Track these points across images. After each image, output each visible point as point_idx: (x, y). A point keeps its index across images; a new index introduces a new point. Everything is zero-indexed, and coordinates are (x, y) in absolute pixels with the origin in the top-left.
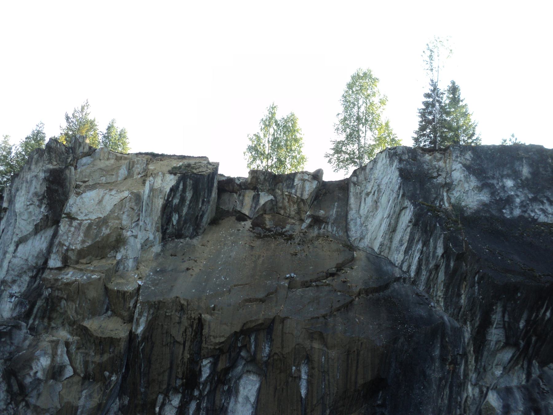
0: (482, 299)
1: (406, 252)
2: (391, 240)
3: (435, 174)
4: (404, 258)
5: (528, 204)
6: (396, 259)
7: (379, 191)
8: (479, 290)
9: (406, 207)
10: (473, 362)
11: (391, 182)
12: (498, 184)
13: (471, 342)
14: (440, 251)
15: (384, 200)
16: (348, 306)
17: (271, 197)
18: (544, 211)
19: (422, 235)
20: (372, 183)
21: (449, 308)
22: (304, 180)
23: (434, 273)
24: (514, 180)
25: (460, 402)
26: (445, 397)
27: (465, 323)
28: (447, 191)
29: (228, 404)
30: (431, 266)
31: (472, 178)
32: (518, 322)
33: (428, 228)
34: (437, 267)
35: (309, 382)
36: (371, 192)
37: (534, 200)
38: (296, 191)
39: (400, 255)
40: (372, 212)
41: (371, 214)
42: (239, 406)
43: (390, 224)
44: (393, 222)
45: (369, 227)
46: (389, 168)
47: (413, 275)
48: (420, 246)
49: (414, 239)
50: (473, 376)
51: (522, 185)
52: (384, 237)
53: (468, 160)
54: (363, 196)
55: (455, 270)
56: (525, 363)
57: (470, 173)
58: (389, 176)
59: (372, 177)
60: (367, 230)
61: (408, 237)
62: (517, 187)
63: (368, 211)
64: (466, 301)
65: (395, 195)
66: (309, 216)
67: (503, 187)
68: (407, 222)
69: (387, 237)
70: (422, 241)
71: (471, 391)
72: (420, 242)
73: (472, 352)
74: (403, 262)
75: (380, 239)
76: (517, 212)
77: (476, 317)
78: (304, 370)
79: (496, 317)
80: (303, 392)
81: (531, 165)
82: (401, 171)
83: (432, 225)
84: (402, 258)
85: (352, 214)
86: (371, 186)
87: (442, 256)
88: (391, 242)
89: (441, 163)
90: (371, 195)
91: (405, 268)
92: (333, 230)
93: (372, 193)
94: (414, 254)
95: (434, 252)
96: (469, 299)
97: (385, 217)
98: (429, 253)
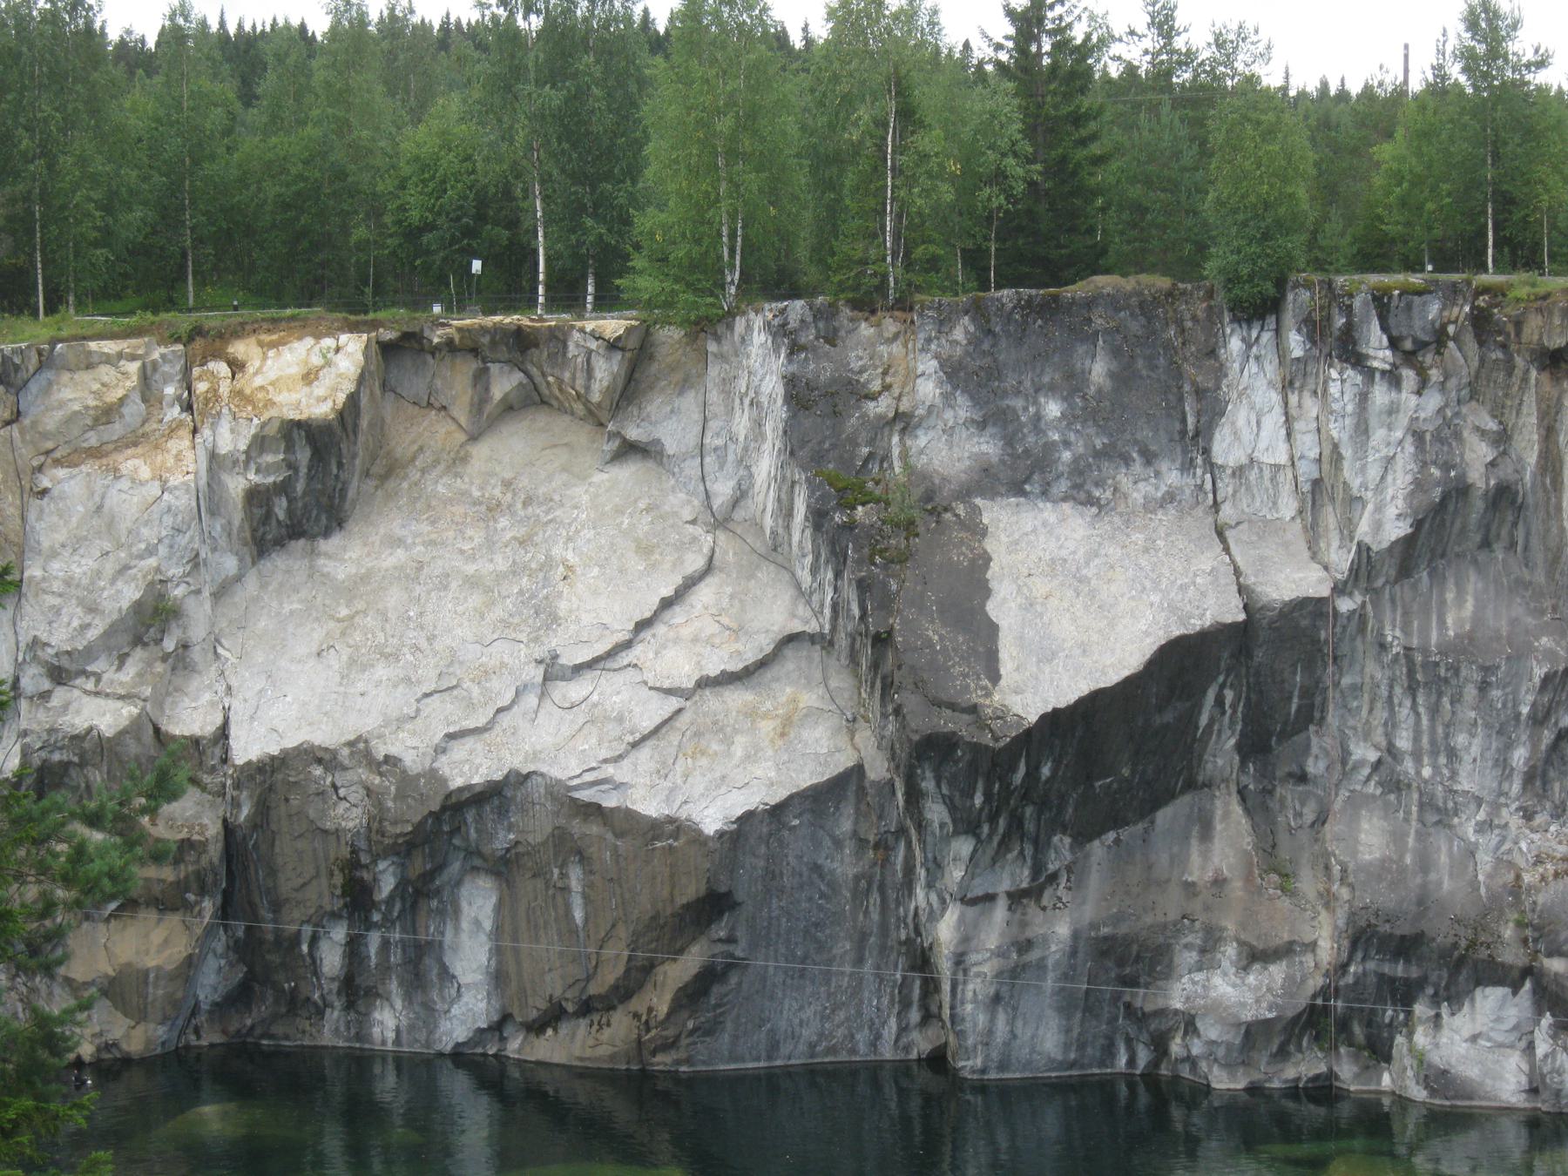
3: (876, 386)
5: (1090, 465)
12: (1026, 409)
17: (518, 377)
24: (1065, 399)
25: (906, 916)
26: (871, 908)
28: (903, 431)
29: (443, 934)
31: (961, 400)
32: (972, 797)
38: (574, 378)
42: (464, 937)
44: (783, 496)
48: (830, 575)
51: (1087, 412)
53: (957, 343)
56: (1029, 850)
57: (955, 388)
62: (1069, 418)
67: (1038, 417)
79: (928, 784)
81: (1116, 352)
82: (790, 382)
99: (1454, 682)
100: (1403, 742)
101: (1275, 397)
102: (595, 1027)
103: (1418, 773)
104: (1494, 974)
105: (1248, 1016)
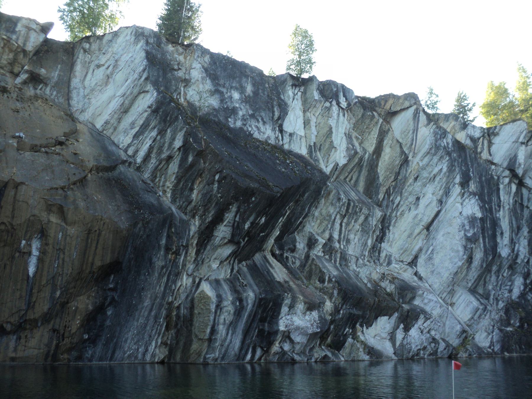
0: (221, 197)
1: (136, 136)
2: (119, 120)
3: (176, 67)
4: (132, 141)
5: (247, 119)
6: (121, 141)
7: (115, 66)
8: (219, 188)
9: (147, 92)
10: (194, 254)
11: (132, 61)
12: (227, 93)
13: (196, 235)
14: (178, 143)
15: (119, 77)
16: (82, 182)
18: (258, 129)
19: (160, 123)
20: (108, 56)
21: (178, 200)
22: (29, 29)
23: (163, 163)
24: (240, 93)
25: (174, 290)
26: (162, 284)
27: (194, 217)
28: (185, 87)
30: (164, 156)
31: (208, 81)
32: (245, 223)
33: (168, 119)
34: (170, 158)
35: (40, 260)
36: (103, 65)
37: (252, 116)
38: (18, 39)
39: (127, 138)
40: (101, 86)
41: (99, 88)
43: (123, 103)
44: (127, 102)
45: (93, 101)
46: (132, 46)
47: (139, 160)
48: (154, 133)
49: (148, 125)
50: (191, 267)
51: (246, 100)
52: (112, 116)
53: (206, 62)
54: (92, 66)
55: (192, 165)
57: (207, 76)
58: (130, 55)
59: (110, 49)
60: (90, 103)
61: (141, 122)
63: (96, 84)
64: (200, 196)
65: (136, 76)
66: (27, 72)
67: (231, 97)
68: (146, 106)
69: (116, 116)
70: (159, 129)
71: (185, 281)
72: (156, 130)
73: (194, 245)
74: (129, 146)
75: (105, 117)
76: (239, 124)
77: (209, 213)
78: (35, 246)
79: (229, 216)
80: (32, 270)
81: (254, 85)
82: (148, 53)
83: (173, 116)
84: (129, 141)
85: (75, 82)
86: (106, 59)
87: (179, 149)
88: (119, 122)
89: (181, 58)
90: (102, 69)
91: (130, 152)
92: (52, 94)
93: (106, 66)
94: (144, 140)
95: (171, 144)
96: (204, 195)
97: (117, 95)
98: (164, 144)
99: (358, 214)
100: (336, 236)
101: (301, 114)
102: (23, 341)
103: (340, 247)
104: (386, 311)
105: (310, 331)
